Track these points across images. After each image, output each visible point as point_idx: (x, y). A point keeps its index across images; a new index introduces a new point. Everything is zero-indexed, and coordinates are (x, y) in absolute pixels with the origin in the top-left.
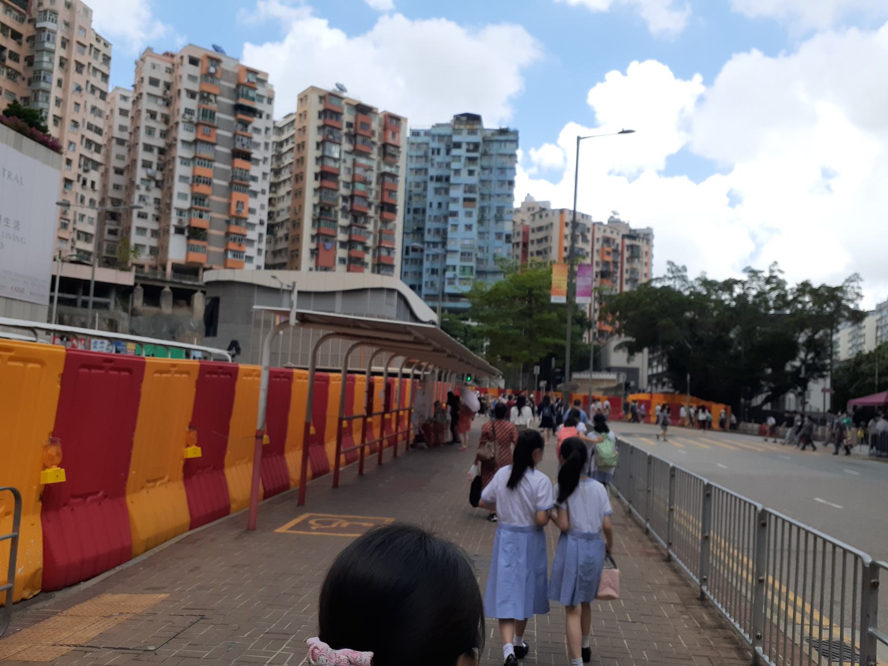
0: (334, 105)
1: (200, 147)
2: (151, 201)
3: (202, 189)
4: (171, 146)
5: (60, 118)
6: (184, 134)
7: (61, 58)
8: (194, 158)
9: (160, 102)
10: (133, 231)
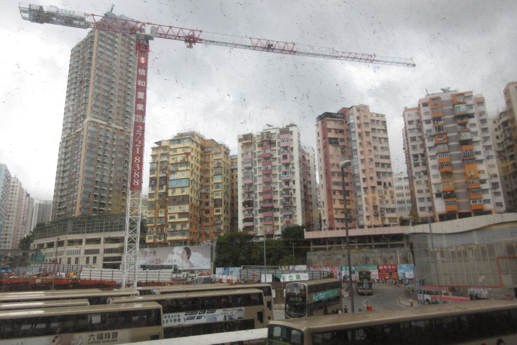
1: (438, 147)
2: (423, 182)
3: (446, 169)
4: (425, 151)
5: (364, 160)
6: (429, 144)
7: (359, 133)
8: (437, 154)
9: (416, 131)
10: (417, 200)
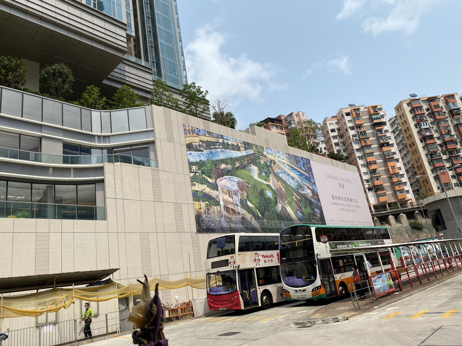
0: (415, 105)
